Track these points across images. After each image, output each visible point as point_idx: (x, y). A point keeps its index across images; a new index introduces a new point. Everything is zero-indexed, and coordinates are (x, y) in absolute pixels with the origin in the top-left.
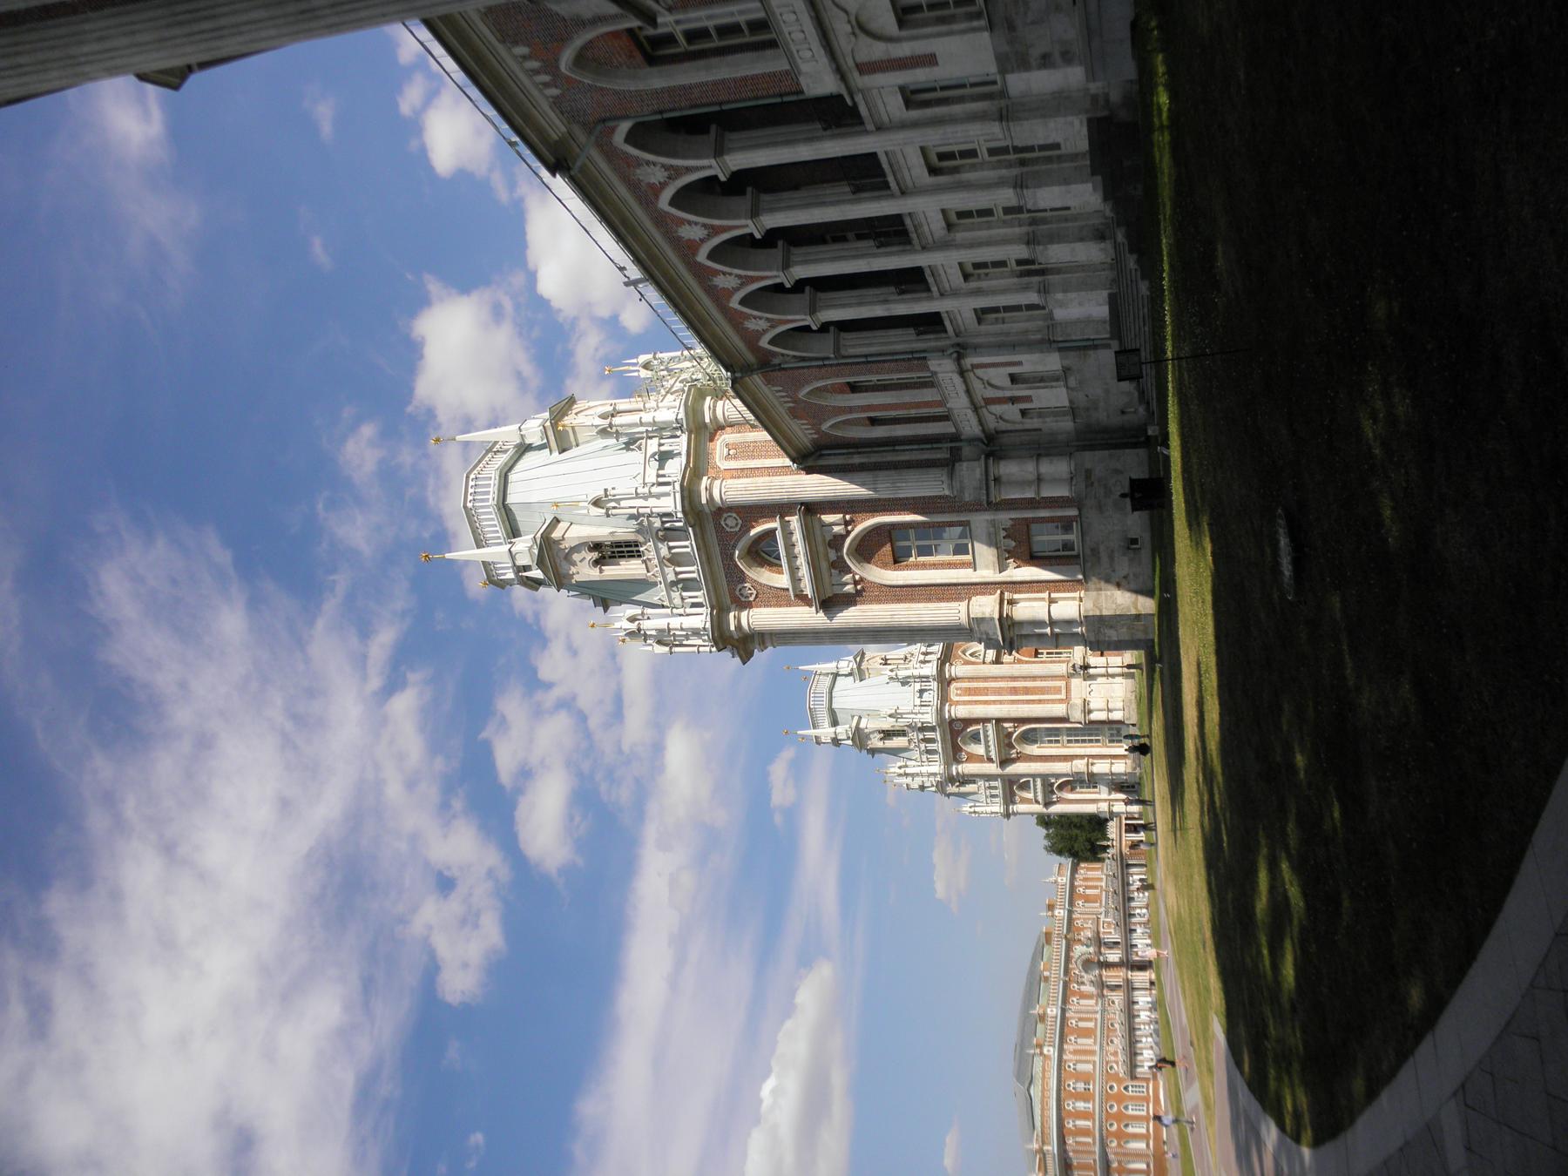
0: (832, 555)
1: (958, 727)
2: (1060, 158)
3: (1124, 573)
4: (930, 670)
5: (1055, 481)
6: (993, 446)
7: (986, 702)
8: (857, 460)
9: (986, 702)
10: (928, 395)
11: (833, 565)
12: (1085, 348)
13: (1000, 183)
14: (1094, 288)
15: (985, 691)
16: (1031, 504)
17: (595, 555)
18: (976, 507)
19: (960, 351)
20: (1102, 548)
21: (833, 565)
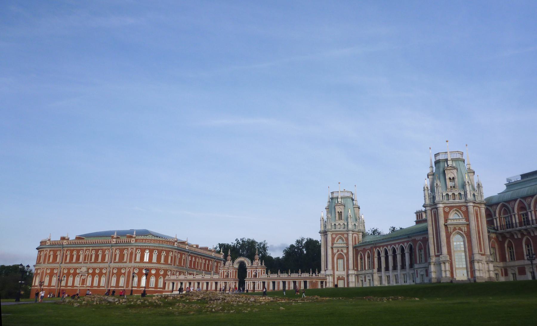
15: (478, 221)
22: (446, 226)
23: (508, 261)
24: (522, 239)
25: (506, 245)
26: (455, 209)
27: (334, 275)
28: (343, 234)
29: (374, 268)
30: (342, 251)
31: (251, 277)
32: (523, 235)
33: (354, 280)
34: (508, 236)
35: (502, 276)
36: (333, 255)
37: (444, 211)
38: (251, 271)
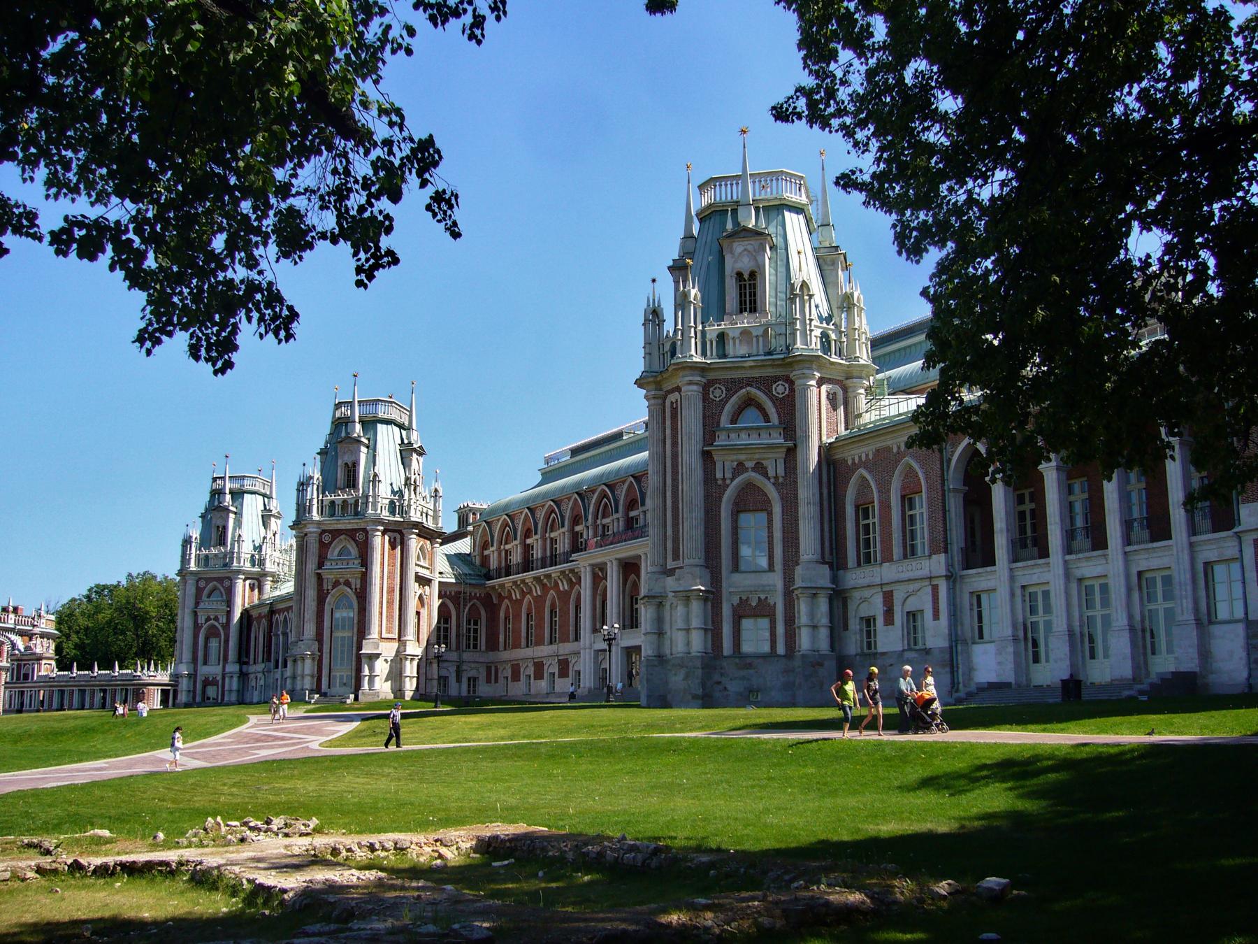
0: (750, 464)
1: (360, 537)
2: (1145, 654)
3: (729, 687)
4: (415, 516)
5: (814, 638)
6: (839, 597)
7: (382, 564)
8: (825, 491)
9: (382, 564)
10: (897, 551)
11: (740, 464)
12: (952, 666)
13: (1130, 617)
14: (1016, 674)
16: (790, 620)
17: (746, 276)
18: (788, 579)
19: (948, 577)
20: (751, 671)
21: (740, 464)
22: (319, 576)
23: (501, 647)
24: (520, 602)
25: (502, 615)
26: (342, 537)
27: (195, 675)
28: (220, 580)
29: (269, 660)
30: (216, 619)
31: (18, 679)
32: (523, 594)
33: (235, 687)
34: (505, 594)
35: (488, 681)
36: (197, 627)
37: (321, 542)
38: (19, 666)
